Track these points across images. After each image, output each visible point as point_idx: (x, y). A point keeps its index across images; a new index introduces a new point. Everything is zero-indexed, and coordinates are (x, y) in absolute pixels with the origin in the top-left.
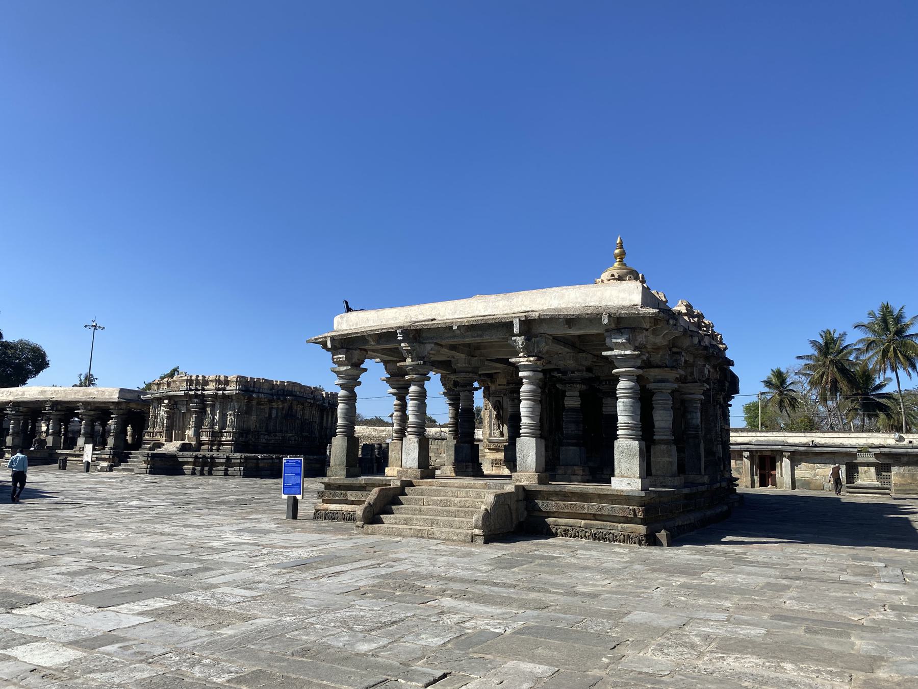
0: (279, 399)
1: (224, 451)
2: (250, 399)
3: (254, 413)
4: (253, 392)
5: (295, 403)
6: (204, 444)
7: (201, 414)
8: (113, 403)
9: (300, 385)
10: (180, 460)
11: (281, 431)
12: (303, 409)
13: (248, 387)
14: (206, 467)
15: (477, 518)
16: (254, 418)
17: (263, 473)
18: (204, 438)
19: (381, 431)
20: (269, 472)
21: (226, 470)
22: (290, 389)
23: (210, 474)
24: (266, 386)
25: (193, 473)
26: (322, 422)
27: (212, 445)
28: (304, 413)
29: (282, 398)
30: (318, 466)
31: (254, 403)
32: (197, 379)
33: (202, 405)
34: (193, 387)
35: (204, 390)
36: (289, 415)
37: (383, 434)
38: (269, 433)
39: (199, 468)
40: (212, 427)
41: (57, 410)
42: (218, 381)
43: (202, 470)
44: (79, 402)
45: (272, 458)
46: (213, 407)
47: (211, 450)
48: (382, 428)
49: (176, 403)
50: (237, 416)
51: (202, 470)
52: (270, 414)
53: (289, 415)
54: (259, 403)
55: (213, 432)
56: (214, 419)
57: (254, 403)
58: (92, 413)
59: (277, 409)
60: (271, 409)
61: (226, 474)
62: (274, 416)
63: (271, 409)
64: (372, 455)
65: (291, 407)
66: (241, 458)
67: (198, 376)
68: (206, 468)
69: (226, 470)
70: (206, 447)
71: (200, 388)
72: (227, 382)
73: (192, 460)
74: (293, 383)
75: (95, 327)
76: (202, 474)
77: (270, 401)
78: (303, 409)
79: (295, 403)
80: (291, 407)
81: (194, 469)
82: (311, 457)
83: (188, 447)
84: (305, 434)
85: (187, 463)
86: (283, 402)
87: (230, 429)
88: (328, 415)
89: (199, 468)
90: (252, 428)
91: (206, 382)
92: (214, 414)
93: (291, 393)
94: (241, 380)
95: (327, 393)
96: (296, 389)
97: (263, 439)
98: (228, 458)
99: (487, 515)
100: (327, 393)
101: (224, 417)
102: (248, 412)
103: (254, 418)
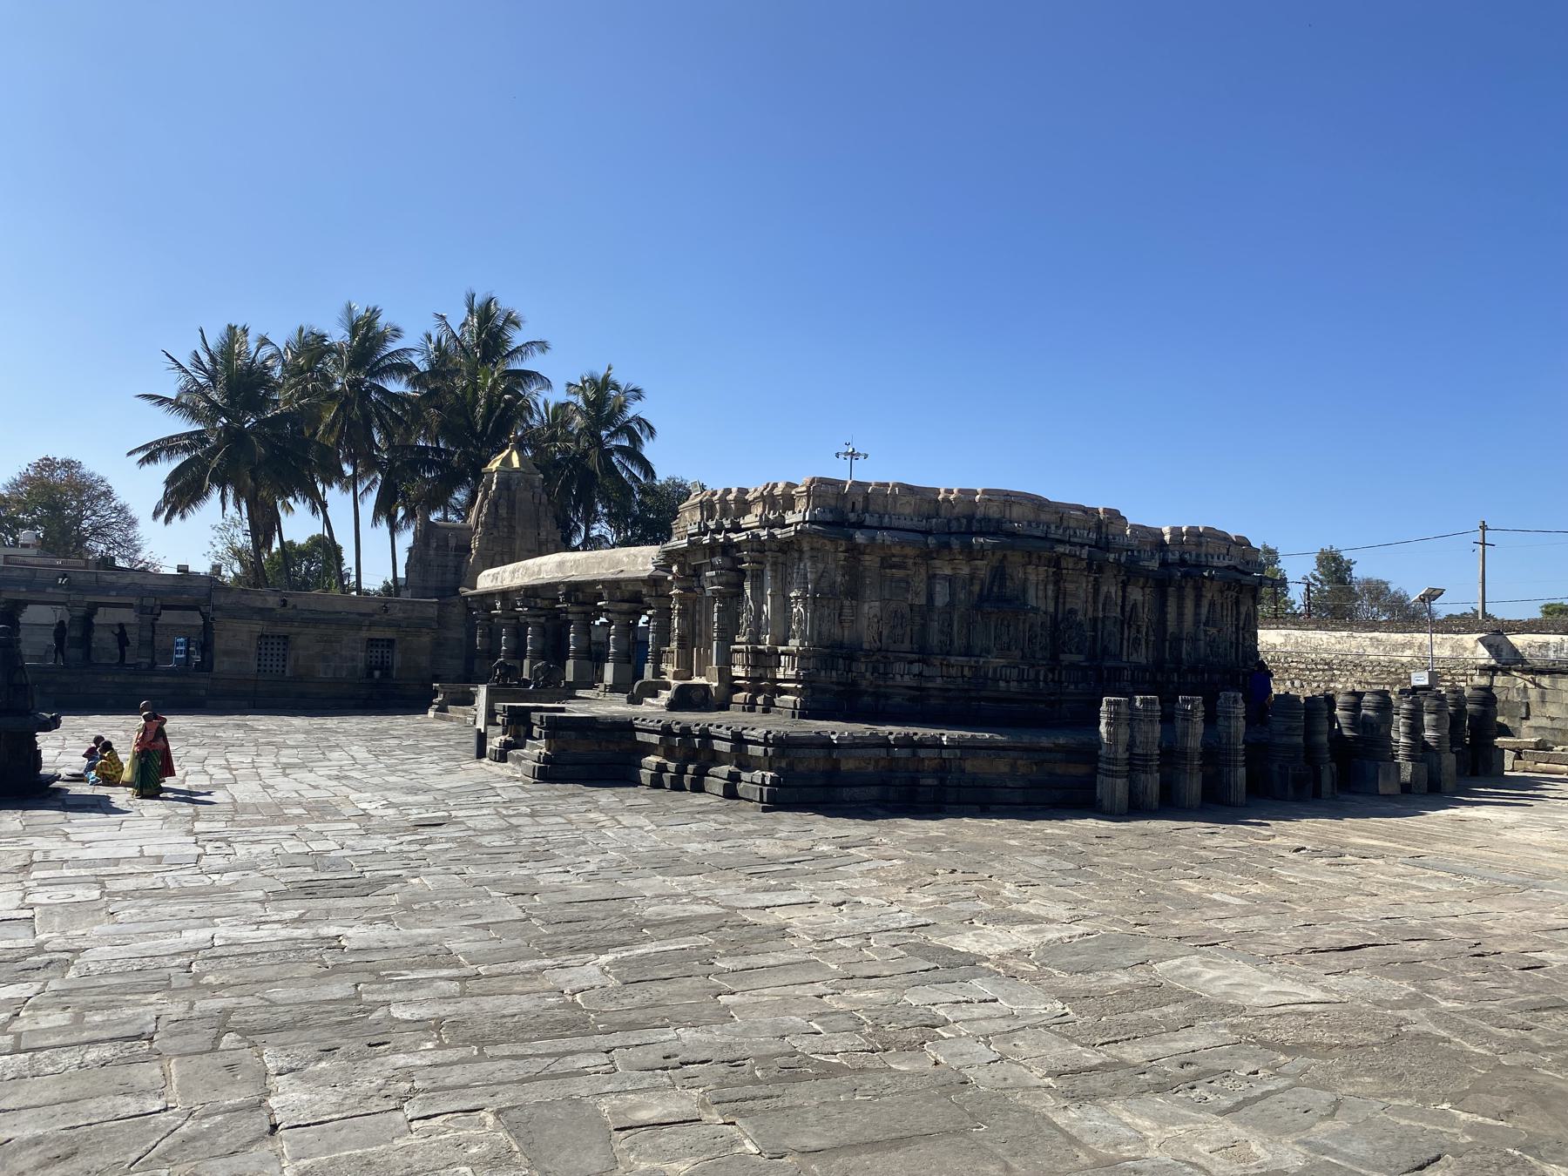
0: (948, 546)
4: (860, 525)
5: (1015, 558)
6: (740, 689)
7: (732, 596)
8: (643, 581)
9: (1040, 503)
10: (640, 737)
11: (968, 652)
12: (1058, 579)
13: (845, 514)
14: (690, 763)
16: (871, 608)
17: (846, 793)
18: (738, 671)
19: (1397, 647)
20: (874, 791)
21: (734, 778)
22: (994, 512)
23: (698, 787)
24: (907, 508)
25: (656, 783)
26: (1162, 621)
27: (757, 691)
28: (1059, 595)
29: (955, 543)
30: (1081, 770)
32: (723, 500)
33: (732, 577)
34: (712, 524)
35: (737, 529)
36: (997, 598)
37: (1406, 656)
38: (923, 653)
39: (672, 766)
40: (755, 639)
41: (577, 603)
42: (769, 499)
43: (681, 771)
44: (594, 582)
45: (884, 743)
46: (758, 578)
47: (751, 706)
48: (1399, 637)
49: (697, 572)
50: (814, 602)
51: (681, 771)
52: (931, 597)
53: (997, 598)
54: (886, 563)
55: (757, 654)
56: (759, 612)
57: (870, 561)
58: (625, 606)
59: (951, 580)
60: (932, 578)
61: (730, 793)
62: (941, 600)
64: (1309, 733)
65: (999, 574)
66: (766, 743)
67: (728, 491)
68: (691, 768)
69: (734, 778)
70: (740, 697)
71: (727, 524)
72: (789, 502)
73: (655, 739)
74: (1008, 494)
75: (852, 454)
76: (677, 786)
77: (927, 556)
78: (1058, 579)
79: (1015, 558)
80: (999, 574)
81: (661, 768)
83: (696, 696)
84: (1066, 658)
85: (648, 749)
89: (672, 766)
90: (868, 639)
91: (744, 506)
92: (759, 602)
93: (993, 527)
94: (822, 489)
95: (1176, 532)
96: (1016, 512)
97: (903, 676)
98: (739, 740)
100: (1176, 532)
101: (784, 605)
102: (854, 592)
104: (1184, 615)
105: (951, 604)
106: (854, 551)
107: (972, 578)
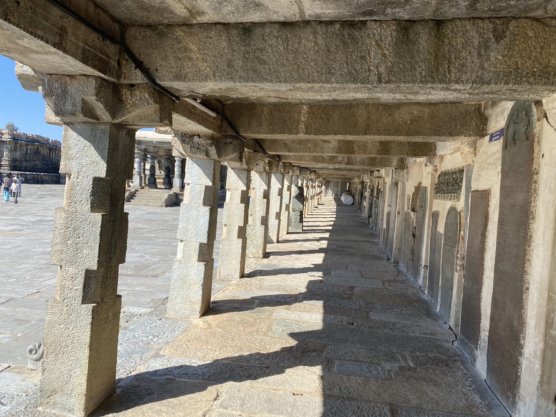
1: (4, 169)
2: (16, 144)
3: (18, 151)
15: (163, 200)
16: (18, 153)
24: (24, 137)
31: (18, 145)
36: (37, 152)
38: (27, 161)
50: (11, 151)
52: (27, 152)
53: (37, 152)
54: (21, 146)
60: (27, 149)
62: (29, 152)
63: (27, 149)
65: (37, 149)
77: (27, 145)
80: (37, 149)
82: (53, 174)
86: (34, 146)
87: (7, 158)
88: (53, 152)
95: (52, 140)
97: (24, 164)
99: (166, 200)
100: (52, 140)
103: (18, 153)
104: (53, 155)
105: (30, 153)
106: (16, 144)
107: (33, 149)
